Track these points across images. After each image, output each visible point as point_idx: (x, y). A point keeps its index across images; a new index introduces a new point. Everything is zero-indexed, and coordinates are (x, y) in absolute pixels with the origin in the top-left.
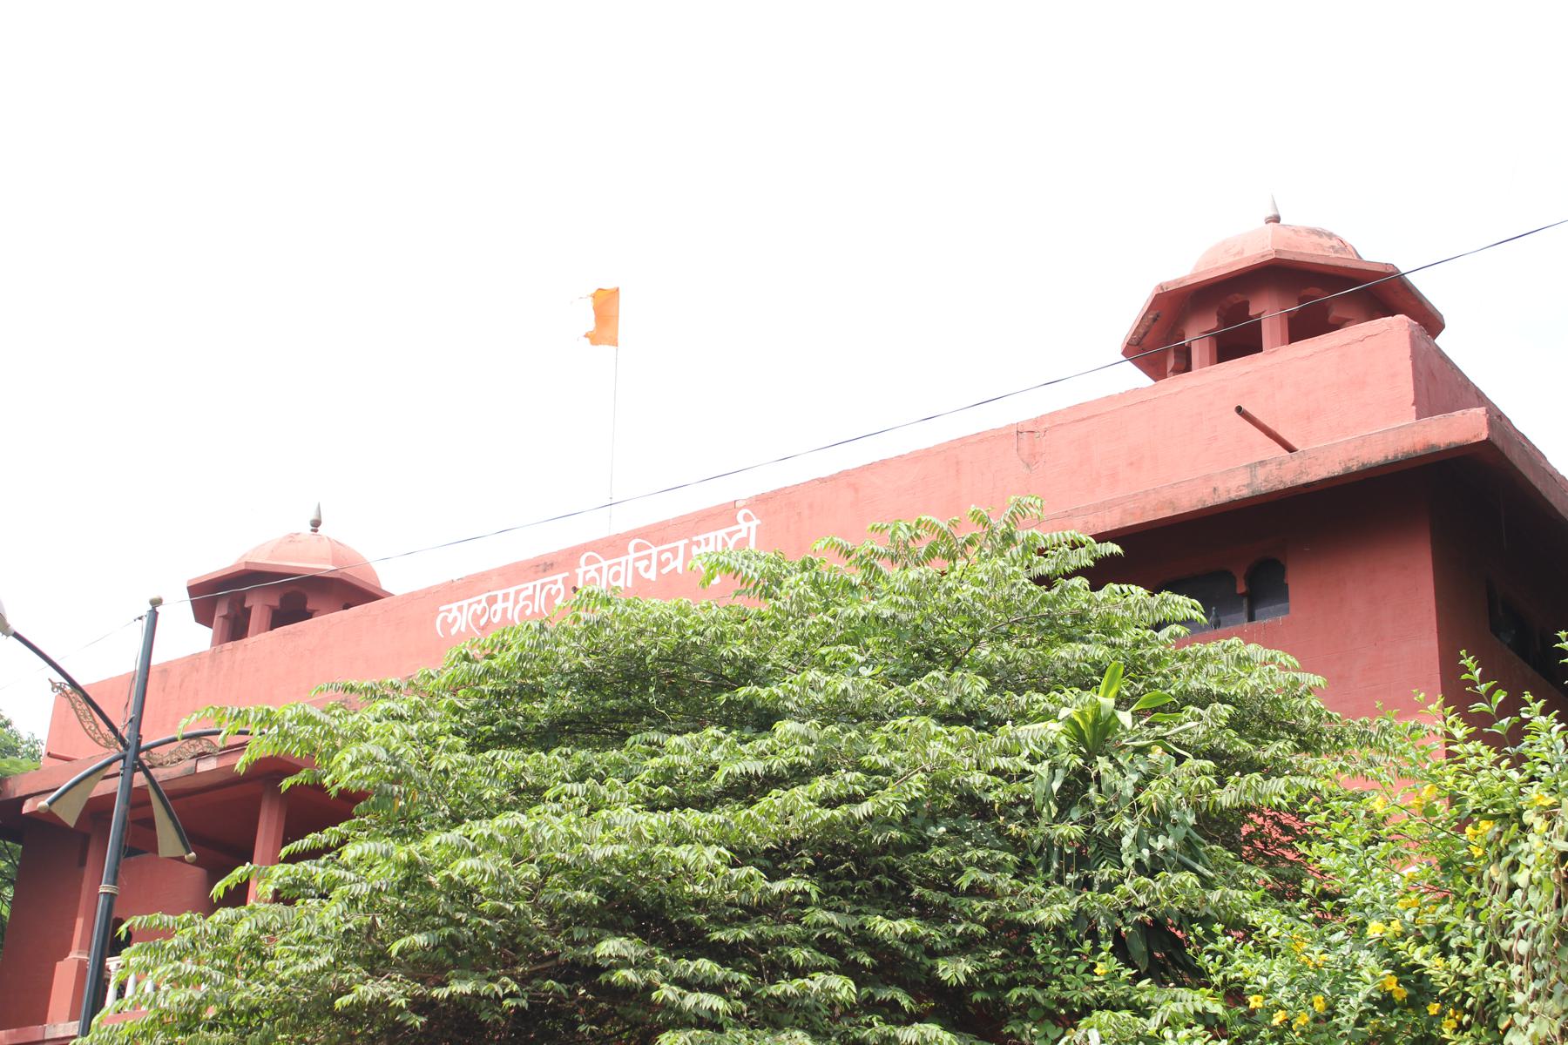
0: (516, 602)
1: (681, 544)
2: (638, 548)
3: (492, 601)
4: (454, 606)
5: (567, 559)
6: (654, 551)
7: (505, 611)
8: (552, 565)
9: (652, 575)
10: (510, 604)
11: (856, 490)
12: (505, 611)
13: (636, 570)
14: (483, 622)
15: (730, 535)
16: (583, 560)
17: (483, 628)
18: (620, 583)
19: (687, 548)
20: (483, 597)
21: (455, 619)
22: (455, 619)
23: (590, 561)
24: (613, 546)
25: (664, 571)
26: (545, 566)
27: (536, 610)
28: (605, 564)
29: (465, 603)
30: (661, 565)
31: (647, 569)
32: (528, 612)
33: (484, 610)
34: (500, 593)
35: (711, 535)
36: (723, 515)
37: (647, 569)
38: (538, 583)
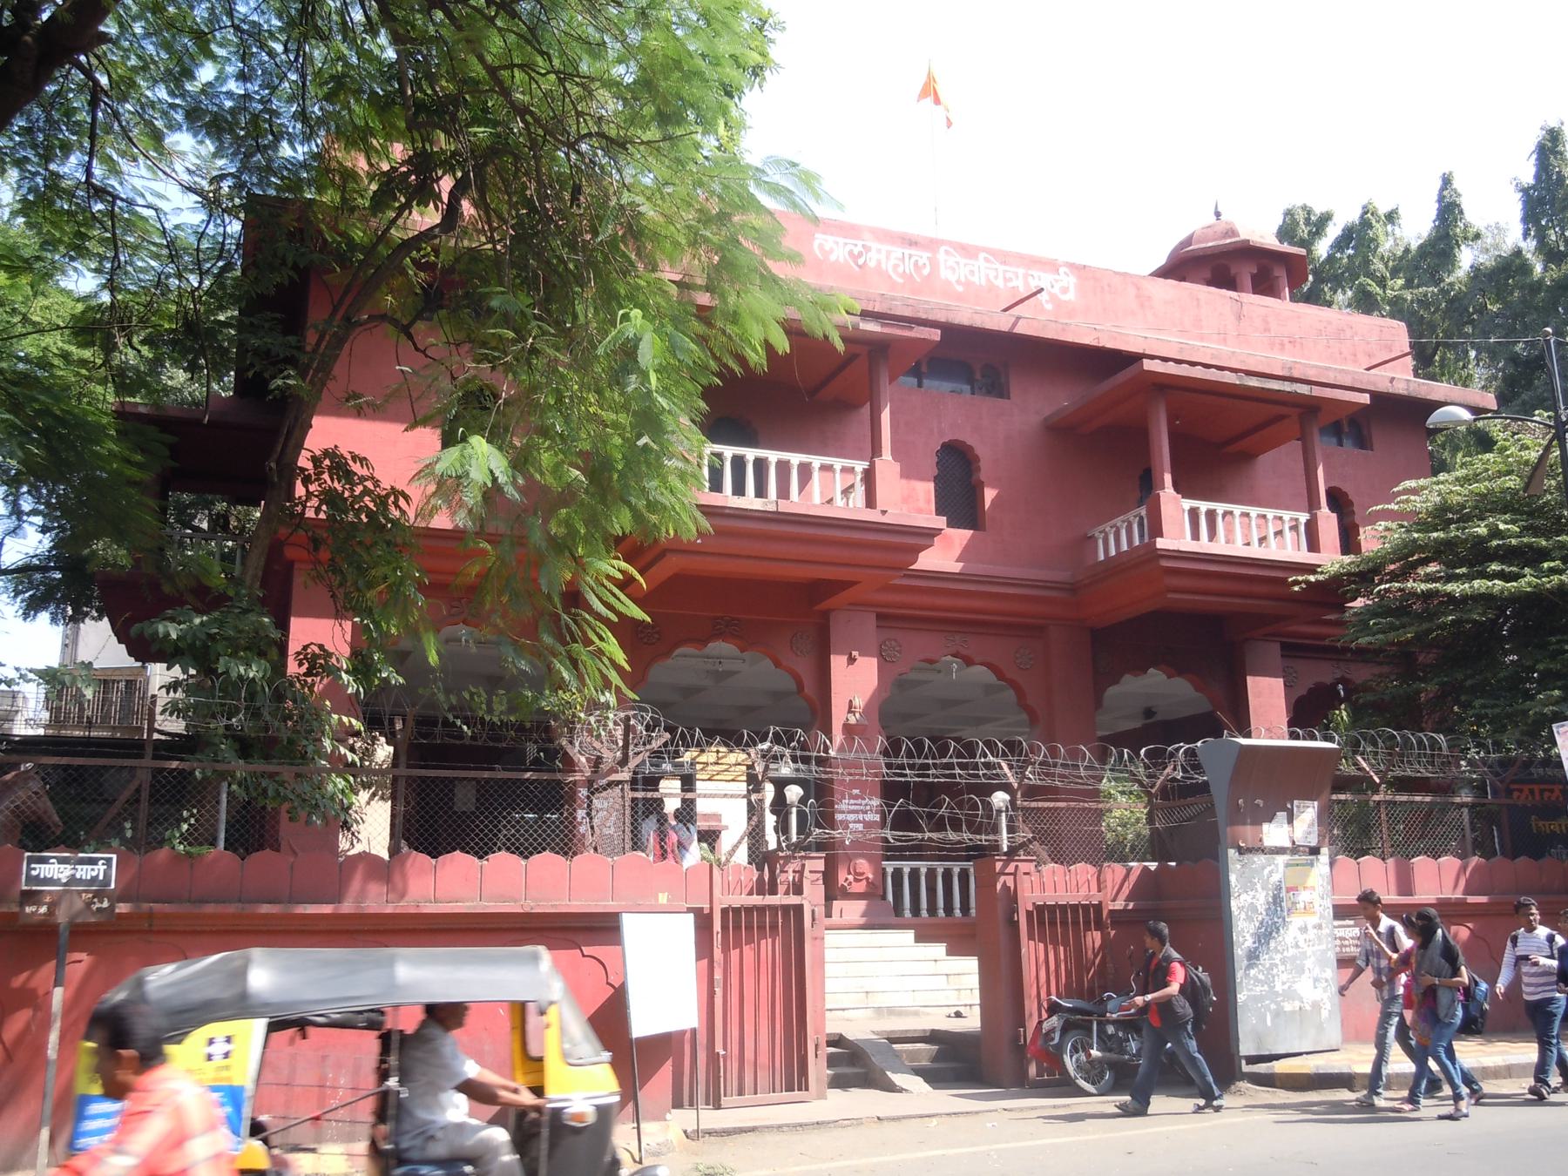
0: (888, 258)
1: (1021, 271)
2: (987, 260)
3: (867, 249)
4: (831, 239)
5: (932, 245)
6: (1002, 268)
7: (879, 263)
8: (916, 243)
9: (1000, 283)
10: (883, 257)
11: (1138, 289)
12: (879, 263)
13: (987, 276)
14: (861, 261)
15: (1057, 281)
16: (943, 249)
17: (860, 267)
18: (975, 279)
19: (1026, 276)
20: (860, 243)
21: (832, 251)
22: (832, 251)
23: (947, 252)
24: (968, 251)
25: (1010, 285)
26: (912, 242)
27: (907, 271)
28: (963, 261)
29: (841, 240)
30: (1006, 280)
31: (996, 277)
32: (901, 270)
33: (860, 254)
34: (874, 245)
35: (1043, 275)
36: (1051, 266)
37: (996, 277)
38: (907, 252)
